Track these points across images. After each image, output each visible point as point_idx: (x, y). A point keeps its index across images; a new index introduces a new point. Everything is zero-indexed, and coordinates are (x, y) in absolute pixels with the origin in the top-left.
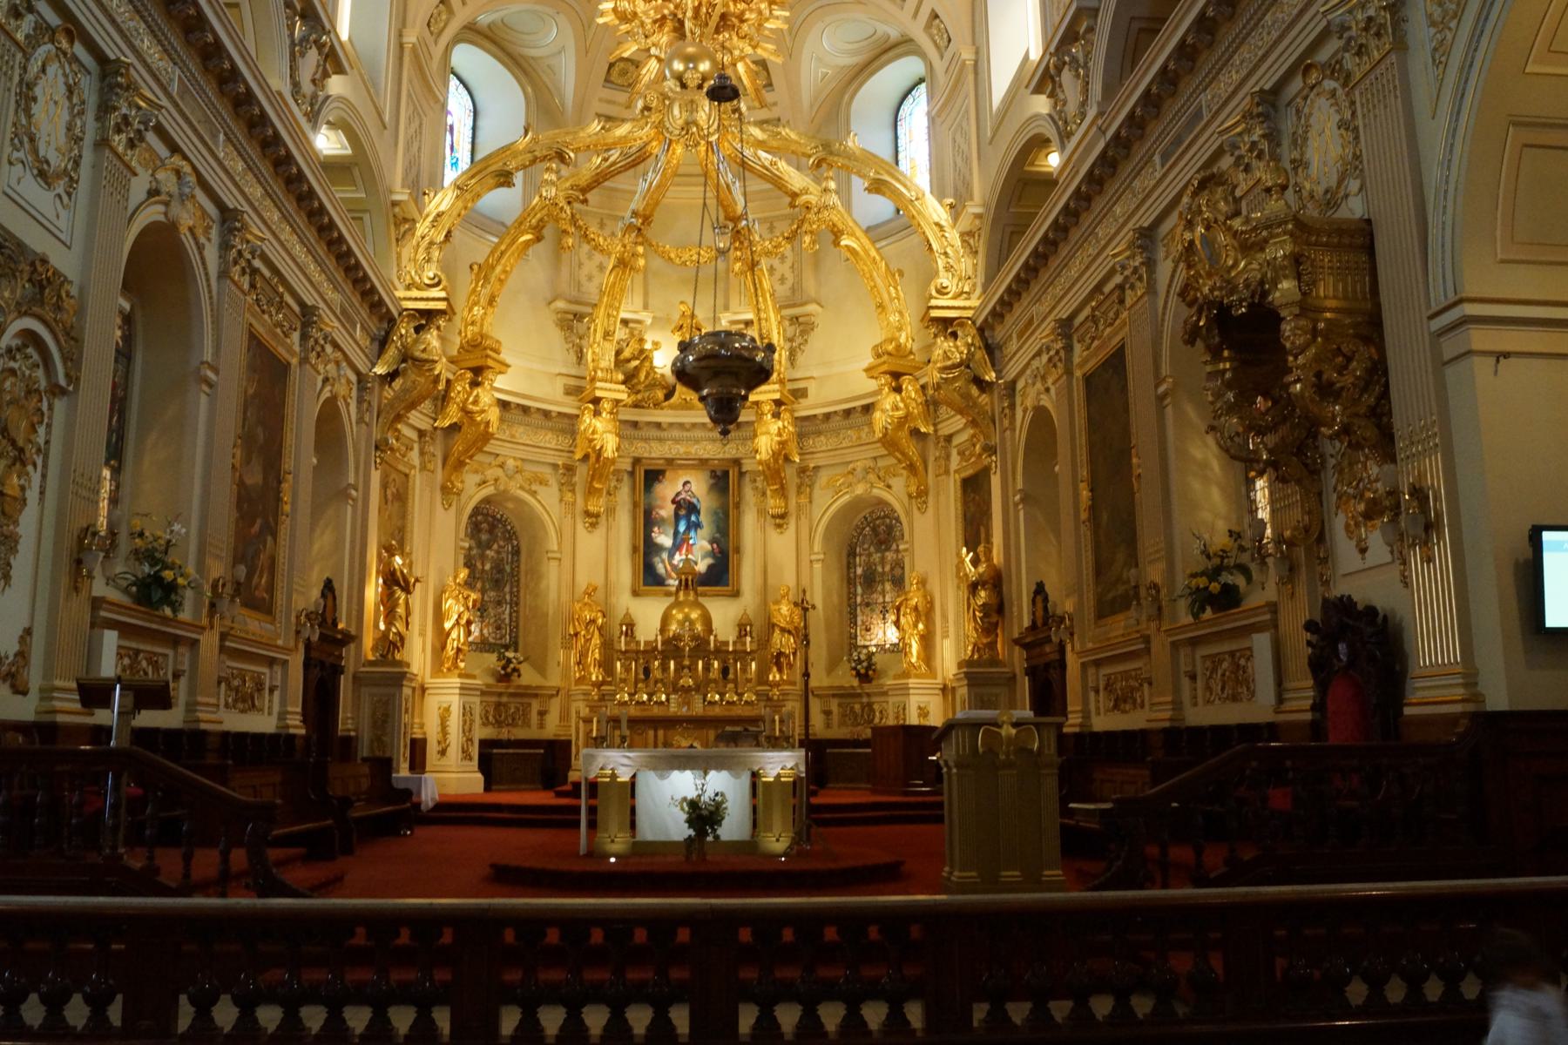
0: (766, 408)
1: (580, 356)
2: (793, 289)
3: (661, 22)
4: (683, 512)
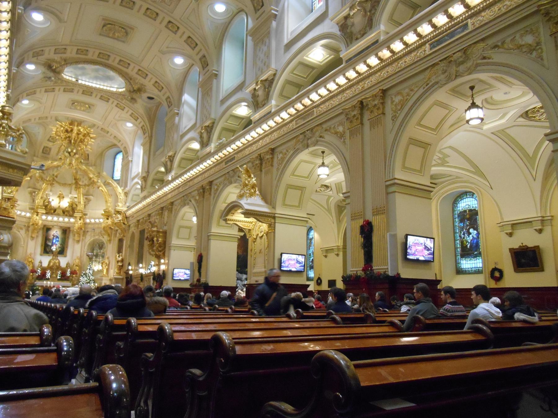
0: (78, 218)
1: (34, 201)
2: (87, 191)
3: (66, 138)
4: (55, 238)
